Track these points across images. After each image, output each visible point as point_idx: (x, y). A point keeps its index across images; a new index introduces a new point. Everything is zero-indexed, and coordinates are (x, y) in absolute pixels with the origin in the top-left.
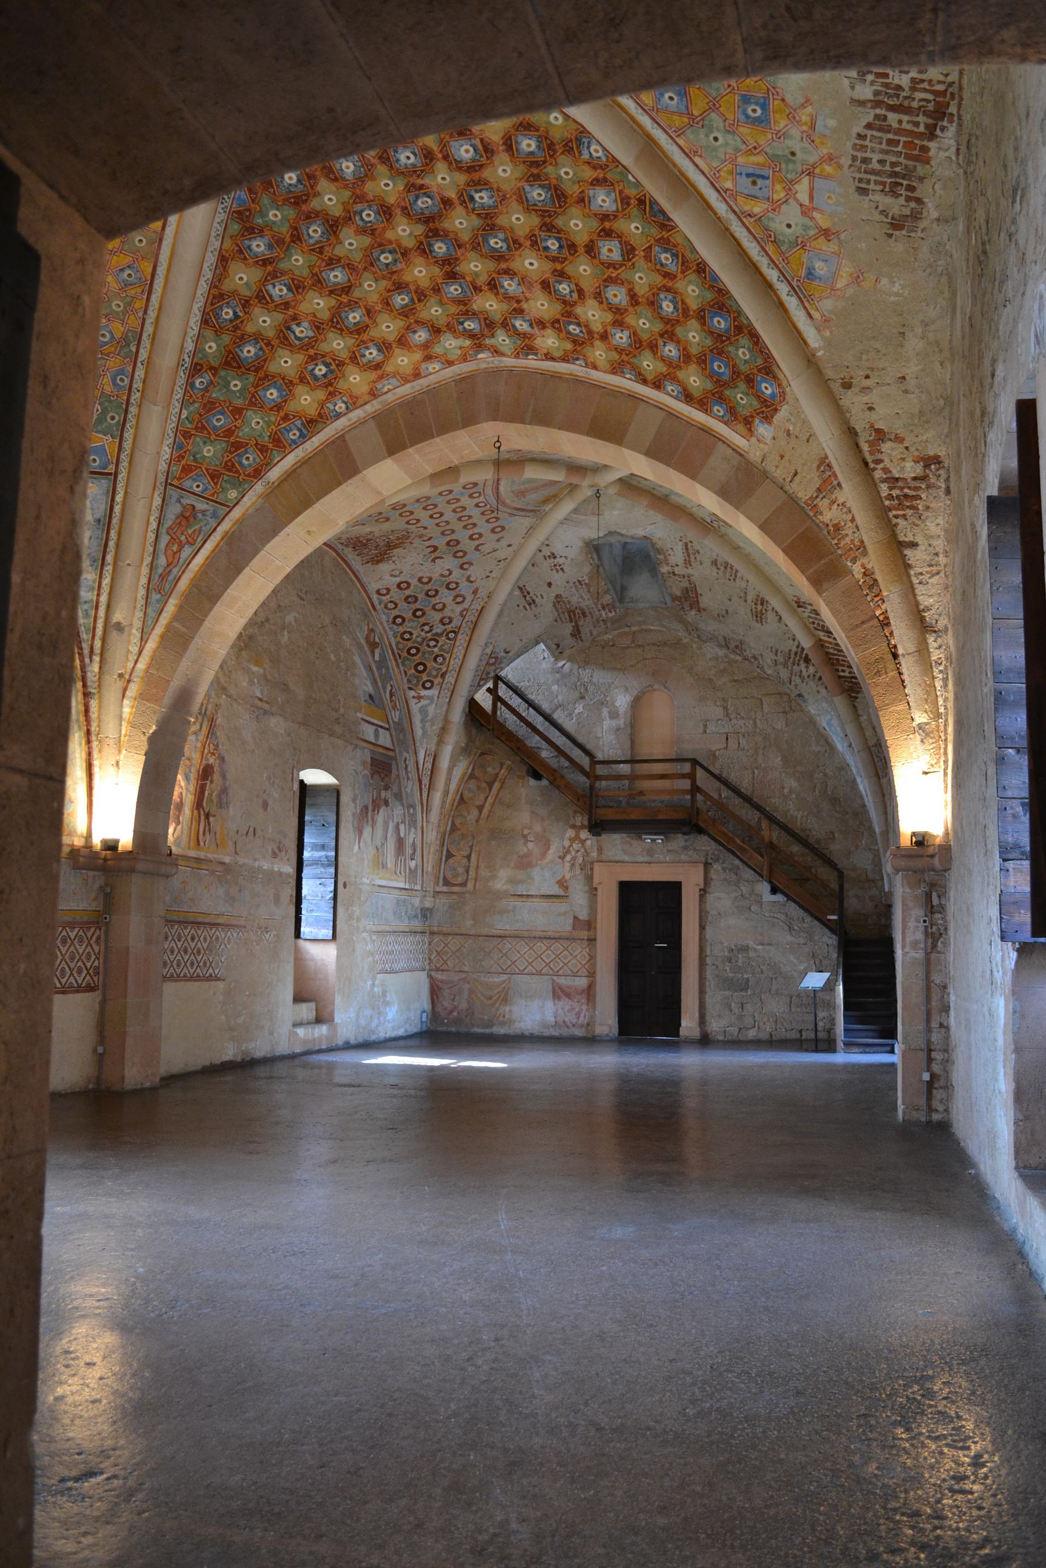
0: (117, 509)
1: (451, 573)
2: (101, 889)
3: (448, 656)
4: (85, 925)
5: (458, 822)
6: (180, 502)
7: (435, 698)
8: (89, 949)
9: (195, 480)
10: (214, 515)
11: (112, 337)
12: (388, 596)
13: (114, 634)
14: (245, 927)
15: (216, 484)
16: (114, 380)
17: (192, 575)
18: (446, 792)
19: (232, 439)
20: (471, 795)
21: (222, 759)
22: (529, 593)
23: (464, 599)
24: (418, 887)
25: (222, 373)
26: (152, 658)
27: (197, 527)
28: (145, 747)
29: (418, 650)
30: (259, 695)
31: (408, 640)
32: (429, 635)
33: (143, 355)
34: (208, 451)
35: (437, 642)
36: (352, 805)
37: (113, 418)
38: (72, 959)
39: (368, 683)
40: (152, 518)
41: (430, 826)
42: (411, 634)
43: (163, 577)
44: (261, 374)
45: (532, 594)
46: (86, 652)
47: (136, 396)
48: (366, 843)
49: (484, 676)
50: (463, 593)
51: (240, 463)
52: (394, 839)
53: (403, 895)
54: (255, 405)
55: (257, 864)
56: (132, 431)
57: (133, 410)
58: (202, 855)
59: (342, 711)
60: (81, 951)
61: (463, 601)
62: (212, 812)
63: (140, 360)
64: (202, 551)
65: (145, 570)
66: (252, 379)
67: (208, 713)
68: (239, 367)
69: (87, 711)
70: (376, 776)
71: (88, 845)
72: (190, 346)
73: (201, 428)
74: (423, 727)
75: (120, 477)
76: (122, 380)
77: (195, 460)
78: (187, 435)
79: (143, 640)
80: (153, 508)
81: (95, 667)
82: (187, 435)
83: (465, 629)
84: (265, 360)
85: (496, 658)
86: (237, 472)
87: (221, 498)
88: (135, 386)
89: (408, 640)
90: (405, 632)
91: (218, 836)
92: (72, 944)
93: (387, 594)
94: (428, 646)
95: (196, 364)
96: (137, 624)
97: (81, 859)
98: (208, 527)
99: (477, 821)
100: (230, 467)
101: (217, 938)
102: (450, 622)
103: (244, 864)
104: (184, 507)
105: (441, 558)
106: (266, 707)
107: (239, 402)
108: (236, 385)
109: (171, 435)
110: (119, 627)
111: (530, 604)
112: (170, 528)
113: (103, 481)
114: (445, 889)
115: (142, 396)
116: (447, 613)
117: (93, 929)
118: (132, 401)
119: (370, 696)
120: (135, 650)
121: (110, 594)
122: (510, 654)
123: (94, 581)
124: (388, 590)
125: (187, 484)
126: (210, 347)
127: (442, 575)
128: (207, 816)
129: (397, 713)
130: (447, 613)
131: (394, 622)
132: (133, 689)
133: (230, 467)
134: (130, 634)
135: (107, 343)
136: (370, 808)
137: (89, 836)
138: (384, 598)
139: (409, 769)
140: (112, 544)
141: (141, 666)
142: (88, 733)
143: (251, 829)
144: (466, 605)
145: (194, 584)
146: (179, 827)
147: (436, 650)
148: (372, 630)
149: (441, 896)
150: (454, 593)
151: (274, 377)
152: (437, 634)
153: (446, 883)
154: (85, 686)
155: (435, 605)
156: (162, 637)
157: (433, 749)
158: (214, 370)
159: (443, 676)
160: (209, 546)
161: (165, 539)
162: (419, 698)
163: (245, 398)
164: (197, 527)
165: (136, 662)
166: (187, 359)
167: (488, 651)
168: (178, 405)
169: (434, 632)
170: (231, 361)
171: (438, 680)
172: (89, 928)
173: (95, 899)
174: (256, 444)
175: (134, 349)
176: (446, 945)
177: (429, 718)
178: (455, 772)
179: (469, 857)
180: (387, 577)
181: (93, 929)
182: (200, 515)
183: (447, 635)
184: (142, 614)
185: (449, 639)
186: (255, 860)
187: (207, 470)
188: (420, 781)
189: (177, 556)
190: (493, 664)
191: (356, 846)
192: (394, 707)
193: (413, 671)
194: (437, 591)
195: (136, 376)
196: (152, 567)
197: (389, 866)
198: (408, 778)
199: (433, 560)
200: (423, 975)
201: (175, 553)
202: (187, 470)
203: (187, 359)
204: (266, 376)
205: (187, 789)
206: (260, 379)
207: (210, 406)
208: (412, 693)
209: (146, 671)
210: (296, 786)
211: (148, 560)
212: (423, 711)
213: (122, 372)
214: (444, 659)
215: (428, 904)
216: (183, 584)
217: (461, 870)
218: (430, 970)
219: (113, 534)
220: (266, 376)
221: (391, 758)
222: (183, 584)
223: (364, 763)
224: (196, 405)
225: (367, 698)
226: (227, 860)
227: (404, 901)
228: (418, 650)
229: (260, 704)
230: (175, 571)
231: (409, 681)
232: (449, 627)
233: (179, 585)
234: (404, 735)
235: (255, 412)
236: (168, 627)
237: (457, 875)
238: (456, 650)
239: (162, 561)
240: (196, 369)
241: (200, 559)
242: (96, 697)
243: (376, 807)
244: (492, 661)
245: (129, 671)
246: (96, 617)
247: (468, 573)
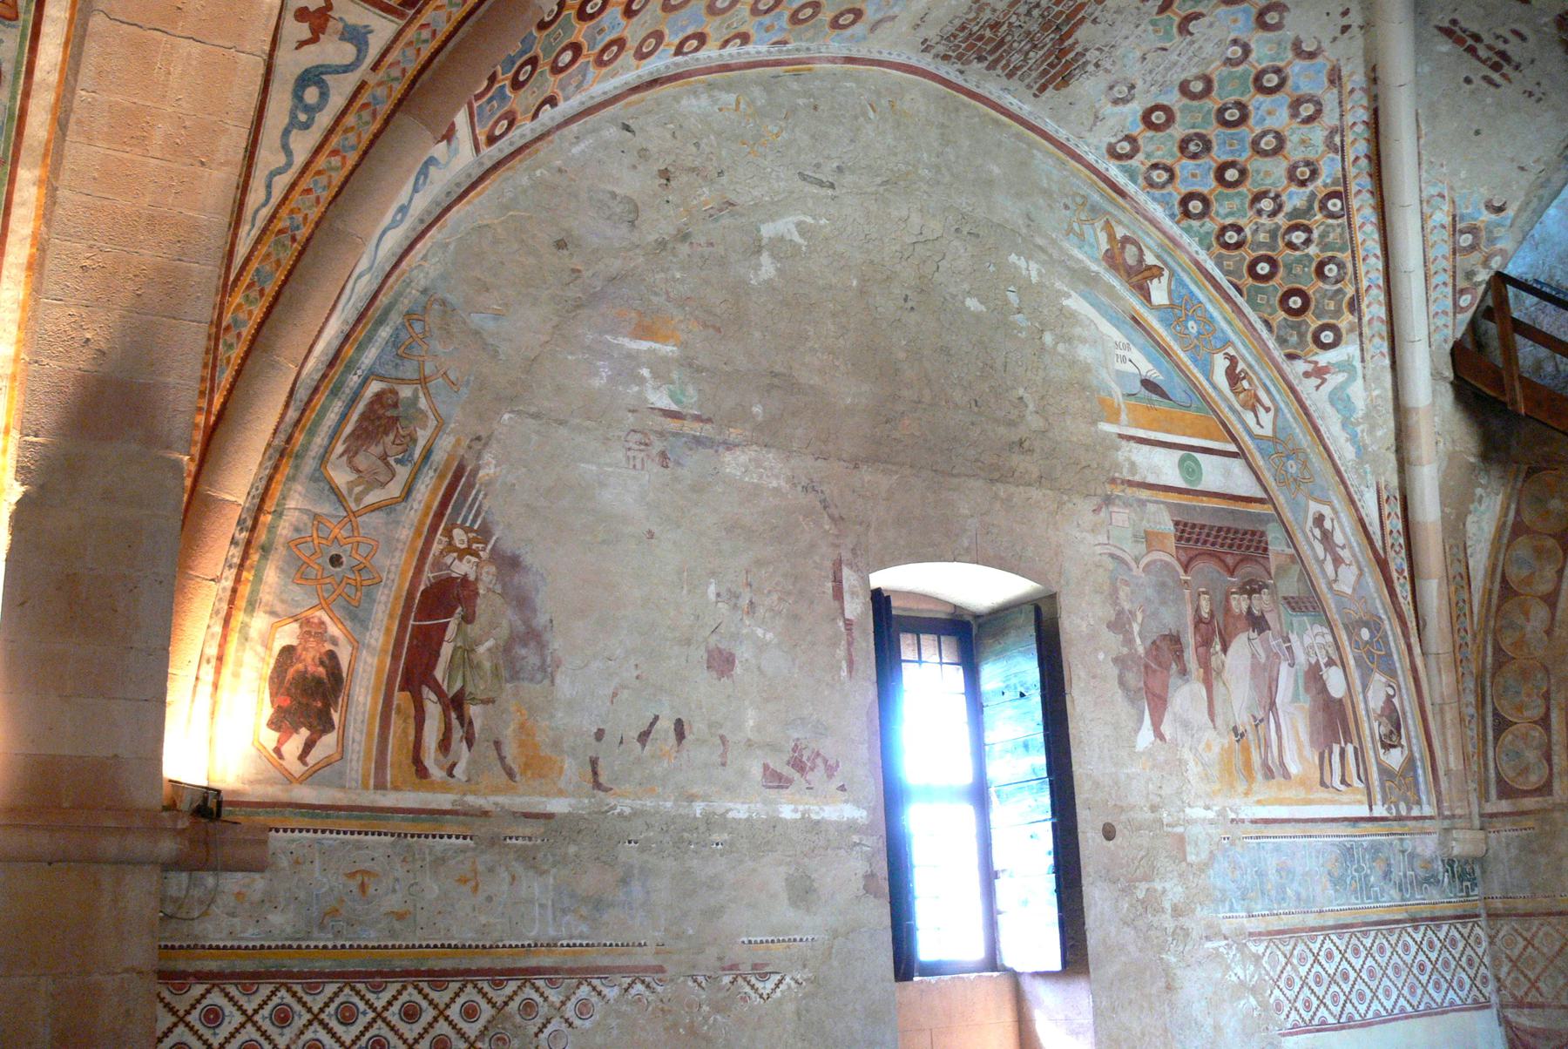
1: (1247, 50)
3: (1345, 256)
5: (1506, 644)
7: (1357, 363)
12: (1140, 156)
14: (660, 969)
18: (1460, 579)
20: (1525, 573)
21: (509, 564)
22: (1477, 38)
23: (1319, 104)
24: (1428, 810)
29: (1272, 262)
30: (662, 400)
31: (1239, 245)
32: (1280, 219)
35: (1308, 230)
36: (1113, 641)
39: (1135, 354)
41: (1432, 661)
42: (1239, 230)
45: (1487, 39)
48: (1186, 725)
49: (1461, 284)
50: (1306, 88)
52: (1306, 702)
53: (1368, 836)
55: (698, 808)
58: (443, 801)
59: (1035, 422)
61: (1319, 112)
62: (478, 687)
64: (46, 28)
67: (439, 456)
70: (1207, 569)
74: (1353, 439)
83: (1360, 182)
85: (1473, 230)
89: (1239, 245)
90: (1224, 230)
91: (510, 751)
93: (1136, 150)
94: (1290, 245)
99: (1549, 632)
101: (528, 1007)
102: (1314, 173)
103: (636, 813)
105: (1197, 16)
106: (707, 430)
111: (1496, 67)
114: (1505, 806)
116: (1294, 152)
119: (1147, 384)
122: (1510, 213)
124: (1130, 139)
127: (1229, 62)
128: (455, 704)
129: (1267, 419)
130: (1294, 152)
131: (1187, 214)
136: (1190, 639)
138: (1134, 162)
139: (1339, 538)
143: (666, 725)
144: (1330, 118)
146: (329, 741)
147: (1313, 250)
148: (1126, 240)
149: (1498, 823)
150: (1282, 98)
152: (1295, 213)
153: (1506, 791)
155: (1255, 143)
157: (1394, 481)
159: (1354, 305)
162: (1320, 372)
167: (1441, 217)
169: (1288, 208)
171: (1345, 321)
176: (1529, 942)
177: (1360, 414)
178: (1471, 528)
179: (1545, 722)
180: (1109, 109)
183: (1323, 207)
185: (1332, 215)
186: (691, 798)
188: (1383, 564)
190: (1473, 247)
191: (1146, 737)
192: (1253, 404)
193: (1282, 315)
194: (1241, 106)
197: (1294, 769)
198: (1338, 561)
199: (1183, 28)
200: (1490, 1016)
205: (357, 645)
208: (1301, 366)
210: (857, 608)
212: (1339, 399)
214: (1341, 266)
215: (1464, 843)
217: (1531, 756)
218: (1503, 1006)
221: (1260, 518)
223: (1150, 539)
225: (1137, 387)
226: (558, 806)
227: (1375, 849)
228: (1272, 262)
229: (672, 425)
231: (1282, 341)
232: (1319, 186)
233: (28, 131)
234: (1305, 464)
237: (1525, 771)
238: (1359, 237)
243: (1215, 631)
244: (1465, 240)
247: (1289, 34)
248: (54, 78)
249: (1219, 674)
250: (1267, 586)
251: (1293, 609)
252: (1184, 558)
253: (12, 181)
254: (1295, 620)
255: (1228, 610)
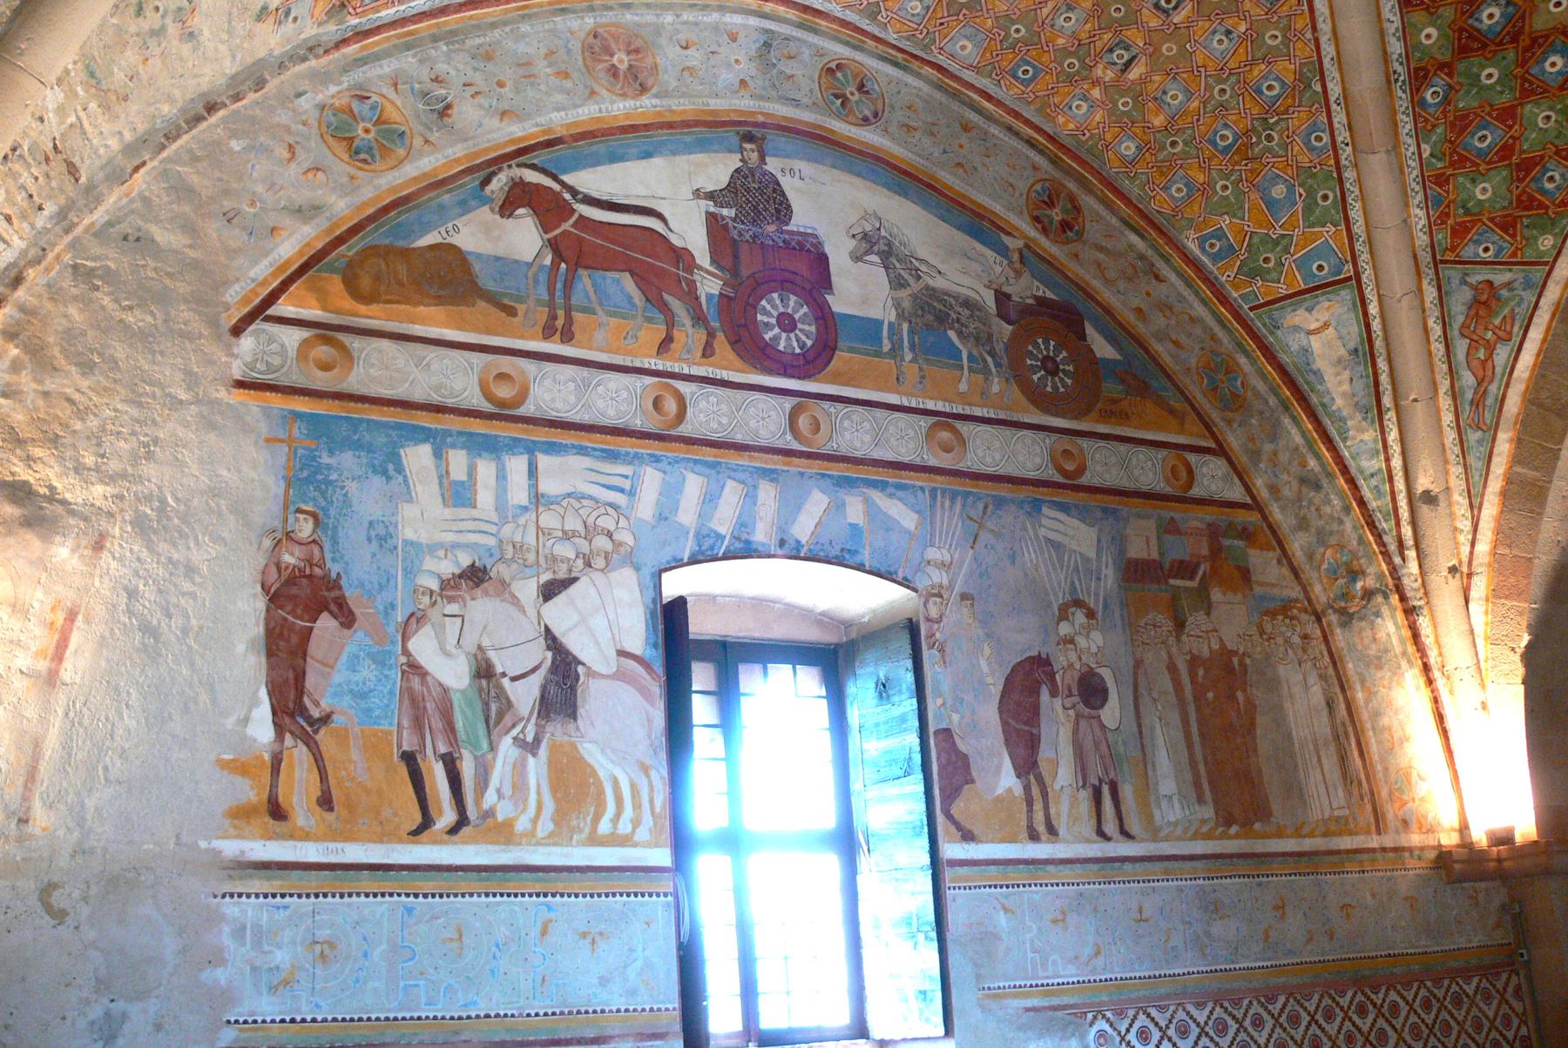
0: (1376, 325)
2: (1504, 908)
4: (1489, 971)
6: (1466, 283)
8: (1505, 1009)
9: (1478, 242)
10: (1528, 285)
11: (1283, 84)
13: (1425, 511)
15: (1513, 236)
16: (1307, 143)
17: (1522, 387)
19: (1515, 159)
25: (1461, 66)
26: (1498, 531)
27: (1506, 311)
28: (1520, 671)
33: (1335, 90)
34: (1483, 192)
37: (1325, 197)
38: (1478, 1027)
40: (1431, 323)
43: (1477, 403)
44: (1524, 41)
46: (1393, 547)
47: (1346, 153)
51: (1544, 192)
54: (1532, 92)
56: (1358, 205)
57: (1349, 175)
60: (1491, 1014)
63: (1332, 99)
64: (1527, 345)
65: (1445, 403)
66: (1511, 55)
68: (1485, 46)
69: (1416, 636)
71: (1466, 844)
72: (1396, 47)
73: (1460, 160)
75: (1364, 279)
76: (1319, 139)
77: (1467, 212)
78: (1441, 180)
79: (1475, 507)
80: (1428, 305)
81: (1413, 567)
82: (1441, 180)
84: (1523, 17)
86: (1541, 206)
87: (1529, 255)
88: (1339, 139)
92: (1473, 1003)
95: (1417, 70)
96: (1457, 484)
97: (1457, 866)
98: (1524, 306)
100: (1527, 203)
104: (1475, 288)
107: (1505, 99)
108: (1490, 76)
109: (1417, 188)
110: (1429, 498)
112: (1463, 326)
113: (1343, 293)
115: (1354, 149)
117: (1504, 976)
118: (1343, 162)
120: (1465, 525)
121: (1404, 453)
123: (1375, 441)
125: (1468, 252)
126: (1428, 36)
132: (1480, 587)
133: (1527, 203)
134: (1450, 505)
135: (1278, 97)
137: (1464, 828)
140: (1384, 378)
141: (1483, 547)
142: (1426, 668)
145: (1532, 400)
151: (1547, 37)
154: (1403, 599)
156: (1504, 494)
158: (1447, 67)
160: (1536, 335)
161: (1461, 346)
163: (1512, 90)
164: (1506, 311)
165: (1473, 544)
166: (1400, 69)
168: (1411, 141)
170: (1469, 43)
172: (1498, 974)
173: (1498, 925)
174: (1558, 152)
175: (1318, 88)
181: (1504, 976)
182: (1504, 293)
184: (1460, 469)
187: (1492, 220)
189: (1489, 364)
195: (1336, 126)
196: (1454, 395)
201: (1484, 362)
202: (1460, 232)
203: (1400, 69)
204: (1534, 41)
206: (1526, 50)
207: (1462, 124)
209: (1493, 553)
211: (1444, 386)
213: (1314, 127)
216: (1513, 404)
219: (1382, 365)
220: (1534, 41)
222: (1513, 404)
224: (1439, 130)
230: (1493, 388)
233: (1506, 408)
235: (1536, 103)
236: (1509, 480)
239: (1468, 379)
240: (1419, 77)
241: (1527, 359)
242: (1425, 611)
245: (1465, 559)
246: (1393, 493)
248: (1526, 375)
253: (1494, 440)
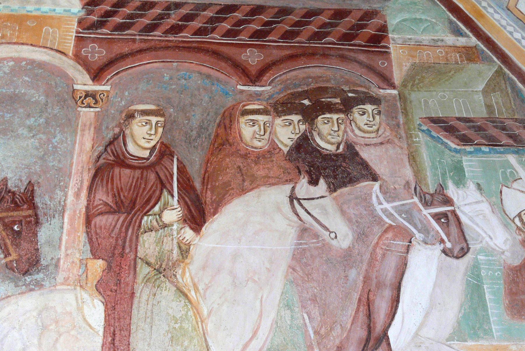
249: (163, 270)
250: (375, 101)
251: (465, 140)
252: (97, 54)
254: (471, 162)
255: (223, 138)
